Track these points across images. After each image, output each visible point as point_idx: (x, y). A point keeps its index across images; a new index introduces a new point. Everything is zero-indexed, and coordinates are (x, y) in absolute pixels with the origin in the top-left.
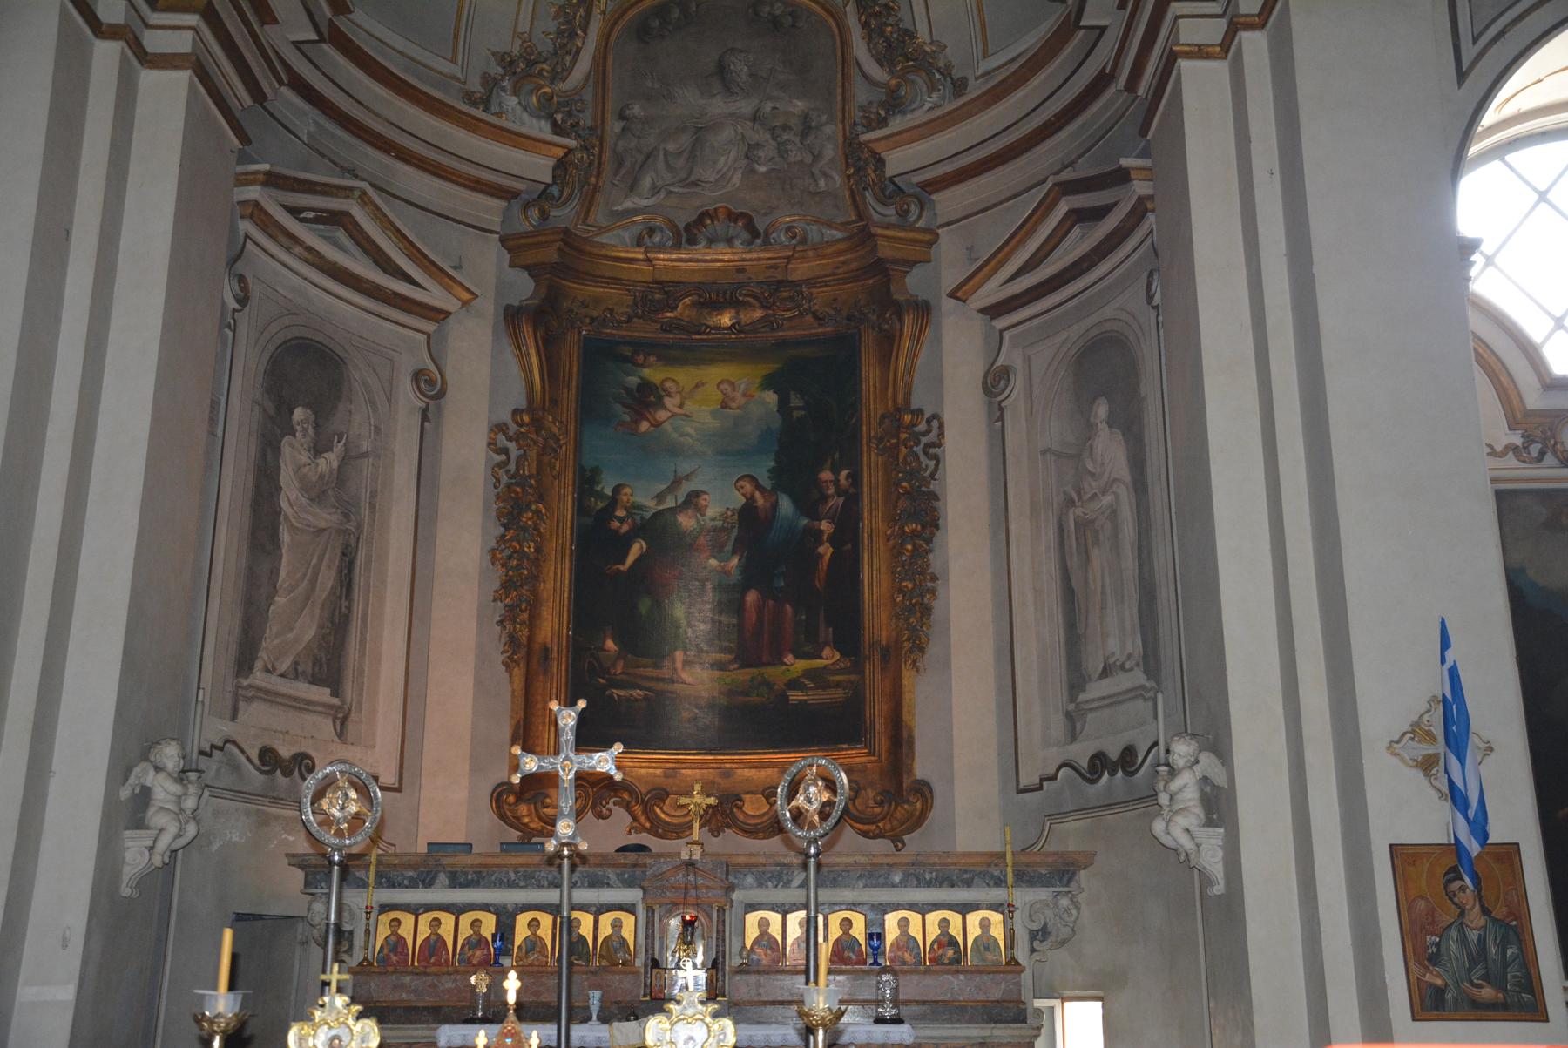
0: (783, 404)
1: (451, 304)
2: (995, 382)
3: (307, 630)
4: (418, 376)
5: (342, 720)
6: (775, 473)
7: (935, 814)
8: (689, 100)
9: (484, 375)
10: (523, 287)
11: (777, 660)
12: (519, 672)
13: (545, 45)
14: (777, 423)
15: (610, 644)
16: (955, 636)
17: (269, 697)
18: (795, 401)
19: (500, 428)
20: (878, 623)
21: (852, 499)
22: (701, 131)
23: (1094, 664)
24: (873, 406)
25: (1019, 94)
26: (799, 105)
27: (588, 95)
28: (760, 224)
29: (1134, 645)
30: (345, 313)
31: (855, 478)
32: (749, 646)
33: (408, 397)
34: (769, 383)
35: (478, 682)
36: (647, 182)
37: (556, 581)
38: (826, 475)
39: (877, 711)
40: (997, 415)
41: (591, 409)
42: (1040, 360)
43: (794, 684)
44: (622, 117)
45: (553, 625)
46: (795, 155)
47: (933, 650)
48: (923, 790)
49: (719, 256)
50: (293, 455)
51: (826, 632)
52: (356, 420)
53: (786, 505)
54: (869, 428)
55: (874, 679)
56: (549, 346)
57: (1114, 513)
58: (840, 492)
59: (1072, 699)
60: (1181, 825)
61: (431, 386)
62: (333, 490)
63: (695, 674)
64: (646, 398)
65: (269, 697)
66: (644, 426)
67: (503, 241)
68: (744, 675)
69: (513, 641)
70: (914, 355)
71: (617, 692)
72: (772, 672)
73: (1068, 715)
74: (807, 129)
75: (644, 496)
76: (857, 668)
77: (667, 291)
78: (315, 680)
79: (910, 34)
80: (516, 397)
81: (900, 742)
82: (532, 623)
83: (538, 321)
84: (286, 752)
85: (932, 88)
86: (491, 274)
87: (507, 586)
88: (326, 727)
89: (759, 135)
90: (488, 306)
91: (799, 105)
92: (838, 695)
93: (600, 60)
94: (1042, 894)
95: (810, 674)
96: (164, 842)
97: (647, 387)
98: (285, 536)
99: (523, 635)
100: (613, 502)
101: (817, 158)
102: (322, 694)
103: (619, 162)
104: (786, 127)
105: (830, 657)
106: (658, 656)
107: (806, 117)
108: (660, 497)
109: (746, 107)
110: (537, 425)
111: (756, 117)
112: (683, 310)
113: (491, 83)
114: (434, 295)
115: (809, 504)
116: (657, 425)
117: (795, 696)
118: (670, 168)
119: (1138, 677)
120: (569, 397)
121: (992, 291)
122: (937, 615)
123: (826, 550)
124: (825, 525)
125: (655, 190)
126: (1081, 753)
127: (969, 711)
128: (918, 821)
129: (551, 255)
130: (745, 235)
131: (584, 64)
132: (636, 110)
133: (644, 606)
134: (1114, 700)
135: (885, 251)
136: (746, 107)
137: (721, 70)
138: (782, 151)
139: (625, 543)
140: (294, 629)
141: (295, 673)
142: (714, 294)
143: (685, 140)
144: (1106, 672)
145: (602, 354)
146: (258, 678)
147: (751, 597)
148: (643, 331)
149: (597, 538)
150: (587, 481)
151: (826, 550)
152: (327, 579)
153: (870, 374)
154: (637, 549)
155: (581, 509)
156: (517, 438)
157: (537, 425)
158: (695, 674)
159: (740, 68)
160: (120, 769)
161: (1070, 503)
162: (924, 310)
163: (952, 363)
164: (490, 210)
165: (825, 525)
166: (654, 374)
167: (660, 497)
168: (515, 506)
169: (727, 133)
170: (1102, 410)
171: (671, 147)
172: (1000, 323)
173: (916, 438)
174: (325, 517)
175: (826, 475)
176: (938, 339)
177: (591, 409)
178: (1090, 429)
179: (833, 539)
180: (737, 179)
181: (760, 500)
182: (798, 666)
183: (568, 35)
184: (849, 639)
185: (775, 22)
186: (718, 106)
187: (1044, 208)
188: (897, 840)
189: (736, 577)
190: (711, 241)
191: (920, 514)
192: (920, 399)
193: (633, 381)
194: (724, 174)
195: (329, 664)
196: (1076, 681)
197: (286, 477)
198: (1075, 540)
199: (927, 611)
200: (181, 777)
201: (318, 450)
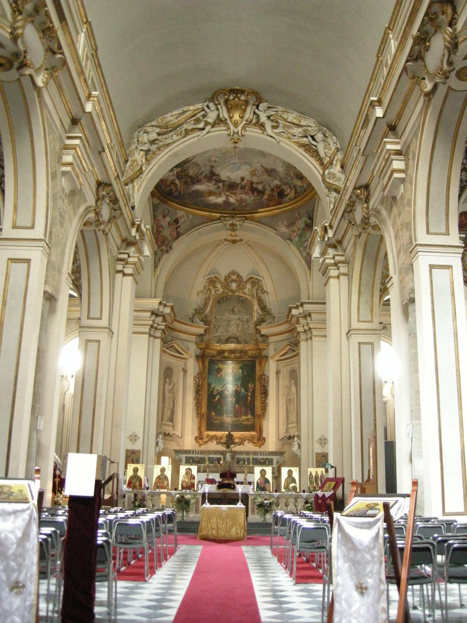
0: (243, 371)
1: (188, 357)
2: (278, 373)
3: (169, 414)
4: (183, 369)
5: (174, 427)
6: (241, 384)
7: (266, 443)
8: (227, 316)
9: (193, 367)
10: (199, 352)
11: (241, 417)
12: (199, 418)
13: (202, 306)
14: (241, 375)
15: (213, 413)
16: (270, 415)
17: (165, 425)
18: (245, 371)
19: (195, 377)
20: (258, 411)
21: (254, 390)
22: (229, 321)
23: (290, 422)
24: (258, 373)
25: (282, 326)
26: (246, 317)
27: (209, 315)
28: (239, 339)
29: (295, 420)
30: (173, 360)
31: (255, 386)
32: (237, 414)
33: (182, 374)
34: (241, 368)
35: (193, 421)
36: (219, 331)
37: (204, 403)
38: (250, 385)
39: (258, 427)
40: (278, 378)
41: (210, 373)
42: (285, 371)
43: (244, 421)
44: (215, 318)
45: (204, 410)
46: (245, 326)
47: (266, 416)
48: (264, 439)
49: (232, 346)
50: (167, 386)
51: (249, 412)
52: (174, 379)
53: (243, 390)
54: (257, 378)
55: (257, 422)
56: (203, 362)
57: (294, 399)
58: (252, 388)
59: (287, 426)
60: (295, 448)
61: (185, 371)
62: (172, 391)
63: (228, 419)
64: (219, 370)
65: (165, 425)
66: (219, 375)
67: (196, 343)
68: (236, 419)
69: (198, 413)
70: (265, 365)
71: (214, 422)
72: (240, 418)
73: (286, 429)
74: (248, 321)
75: (218, 388)
76: (254, 418)
77: (223, 351)
78: (170, 421)
79: (266, 306)
80: (197, 371)
81: (261, 432)
82: (201, 410)
83: (201, 358)
84: (167, 433)
85: (269, 319)
86: (193, 349)
87: (197, 404)
88: (171, 428)
89: (239, 322)
90: (194, 356)
91: (246, 317)
92: (251, 423)
93: (211, 308)
94: (278, 457)
95: (246, 419)
96: (161, 448)
97: (219, 368)
98: (166, 399)
99: (199, 412)
100: (214, 389)
101: (249, 327)
102: (171, 423)
103: (214, 327)
104: (244, 321)
105: (250, 416)
106: (222, 415)
107: (247, 319)
108: (222, 388)
109: (237, 317)
110: (202, 376)
111: (239, 319)
112: (226, 354)
113: (194, 315)
114: (185, 356)
115: (247, 390)
116: (221, 375)
117: (244, 423)
118: (223, 328)
119: (295, 425)
120: (206, 371)
121: (277, 358)
122: (267, 409)
123: (249, 398)
124: (249, 394)
125: (221, 332)
126: (288, 435)
127: (272, 427)
128: (263, 444)
129: (203, 346)
130: (236, 341)
131: (209, 309)
132: (218, 317)
133: (219, 407)
134: (293, 427)
135: (261, 347)
136: (237, 317)
137: (233, 310)
138: (243, 326)
139: (216, 396)
140: (168, 414)
141: (167, 421)
142: (231, 352)
143: (226, 323)
144: (292, 423)
145: (212, 362)
146: (164, 422)
147: (237, 406)
148: (218, 358)
149: (211, 396)
150: (209, 385)
151: (249, 398)
152: (171, 405)
153: (257, 367)
154: (218, 397)
155: (208, 390)
156: (198, 378)
157: (202, 376)
158: (228, 419)
159: (236, 309)
160: (156, 438)
161: (288, 395)
162: (266, 357)
163: (271, 367)
164: (193, 338)
165: (249, 394)
166: (220, 366)
167: (222, 388)
168: (198, 391)
169: (233, 322)
170: (293, 381)
171: (224, 324)
172: (279, 363)
173: (265, 380)
174: (171, 395)
175: (250, 385)
176: (269, 363)
177: (210, 373)
178: (291, 384)
179: (251, 397)
180: (235, 330)
181: (238, 389)
182: (244, 418)
183: (206, 304)
184: (253, 414)
185: (242, 300)
186: (232, 317)
187: (286, 346)
188: (260, 447)
189: (234, 402)
190: (231, 343)
191: (265, 393)
192: (266, 373)
193: (217, 367)
194: (233, 330)
195: (172, 419)
196: (288, 424)
197: (166, 391)
198: (289, 401)
199: (266, 409)
200: (162, 439)
201: (170, 385)
